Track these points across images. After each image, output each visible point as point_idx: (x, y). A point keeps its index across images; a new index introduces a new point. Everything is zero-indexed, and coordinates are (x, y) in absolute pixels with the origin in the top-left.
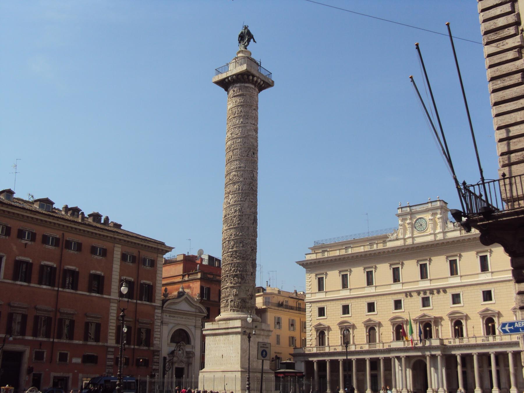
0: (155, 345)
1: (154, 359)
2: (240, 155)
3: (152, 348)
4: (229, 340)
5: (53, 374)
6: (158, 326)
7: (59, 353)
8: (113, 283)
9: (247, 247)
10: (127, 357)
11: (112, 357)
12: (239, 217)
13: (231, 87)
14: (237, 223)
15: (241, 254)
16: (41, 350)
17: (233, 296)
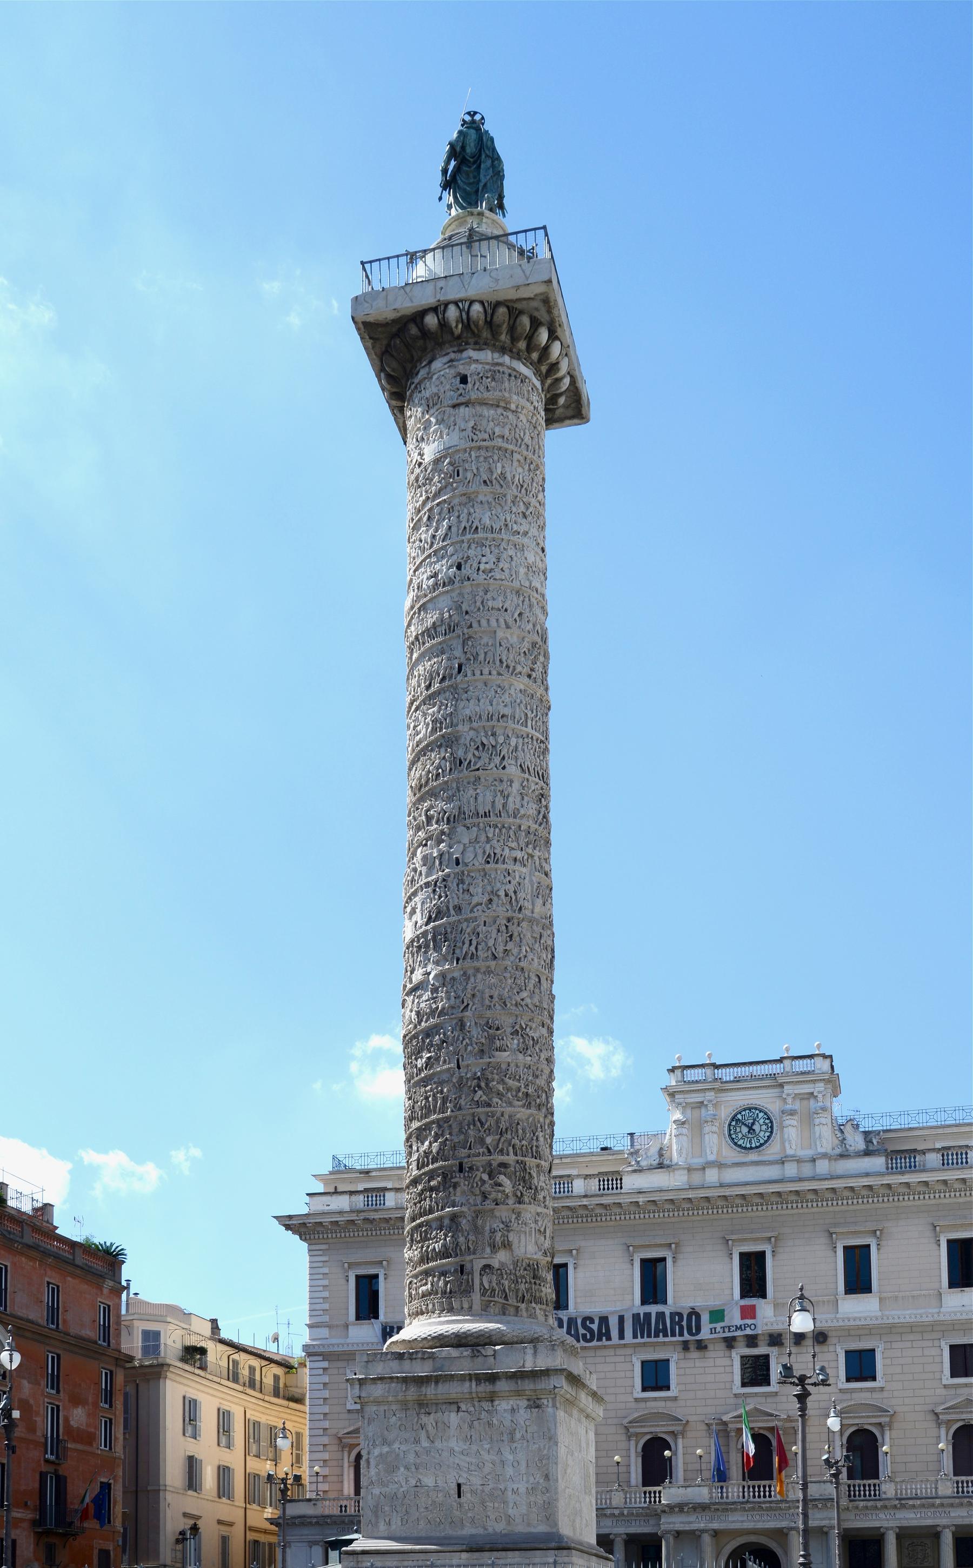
2: (501, 661)
4: (495, 1421)
9: (537, 1058)
12: (507, 926)
13: (445, 359)
14: (501, 948)
15: (519, 1081)
17: (488, 1250)
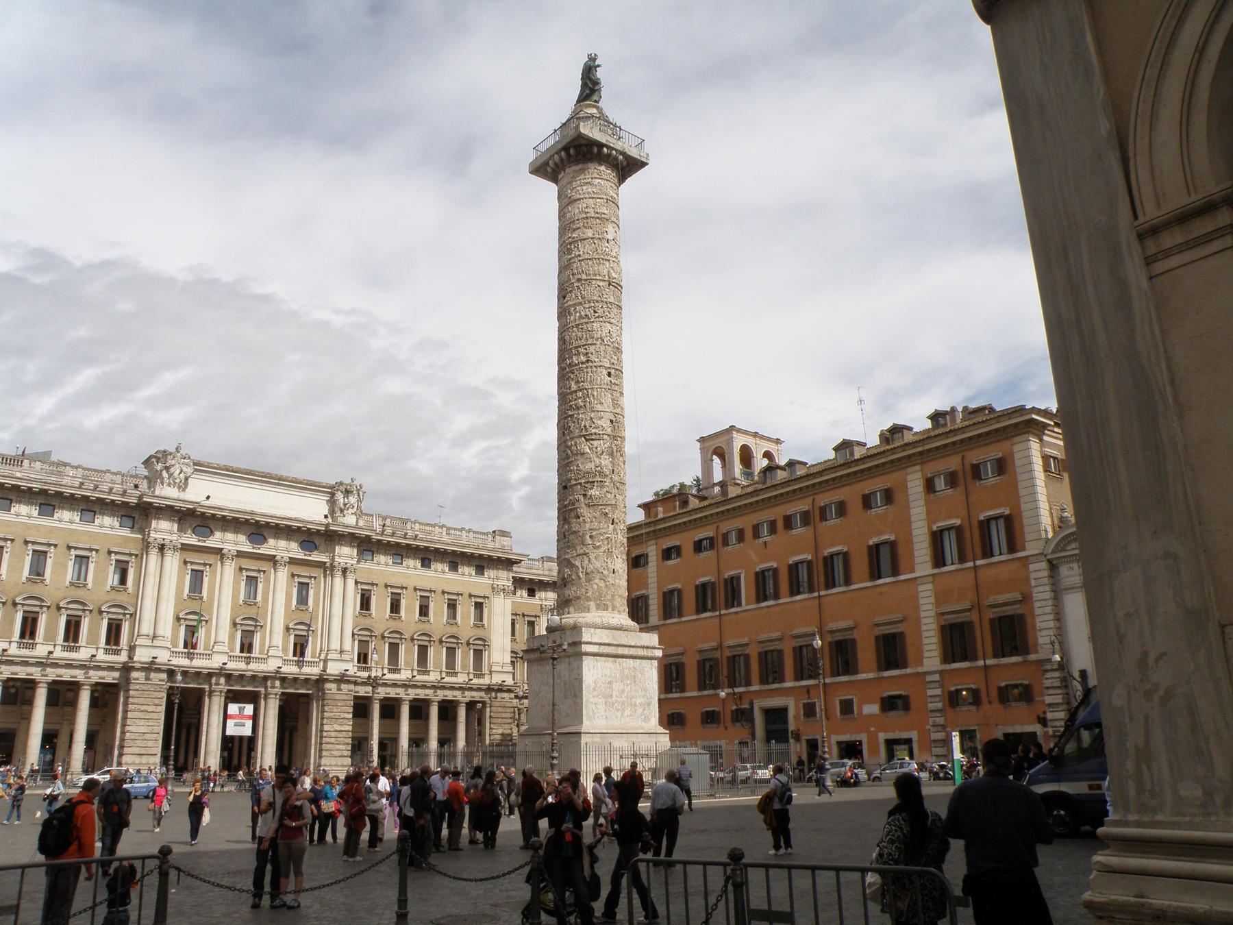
0: (1042, 648)
1: (1045, 681)
3: (1032, 657)
5: (835, 738)
6: (1045, 600)
7: (838, 702)
8: (916, 546)
10: (973, 686)
11: (938, 692)
16: (810, 701)
